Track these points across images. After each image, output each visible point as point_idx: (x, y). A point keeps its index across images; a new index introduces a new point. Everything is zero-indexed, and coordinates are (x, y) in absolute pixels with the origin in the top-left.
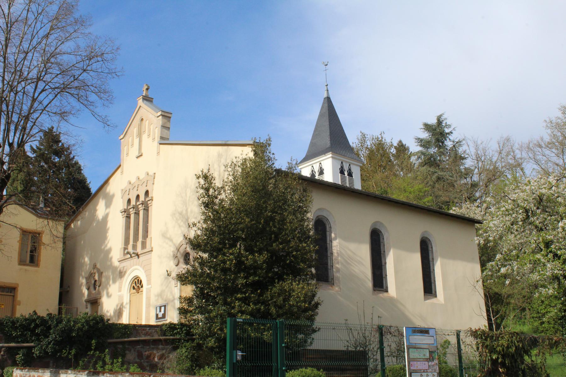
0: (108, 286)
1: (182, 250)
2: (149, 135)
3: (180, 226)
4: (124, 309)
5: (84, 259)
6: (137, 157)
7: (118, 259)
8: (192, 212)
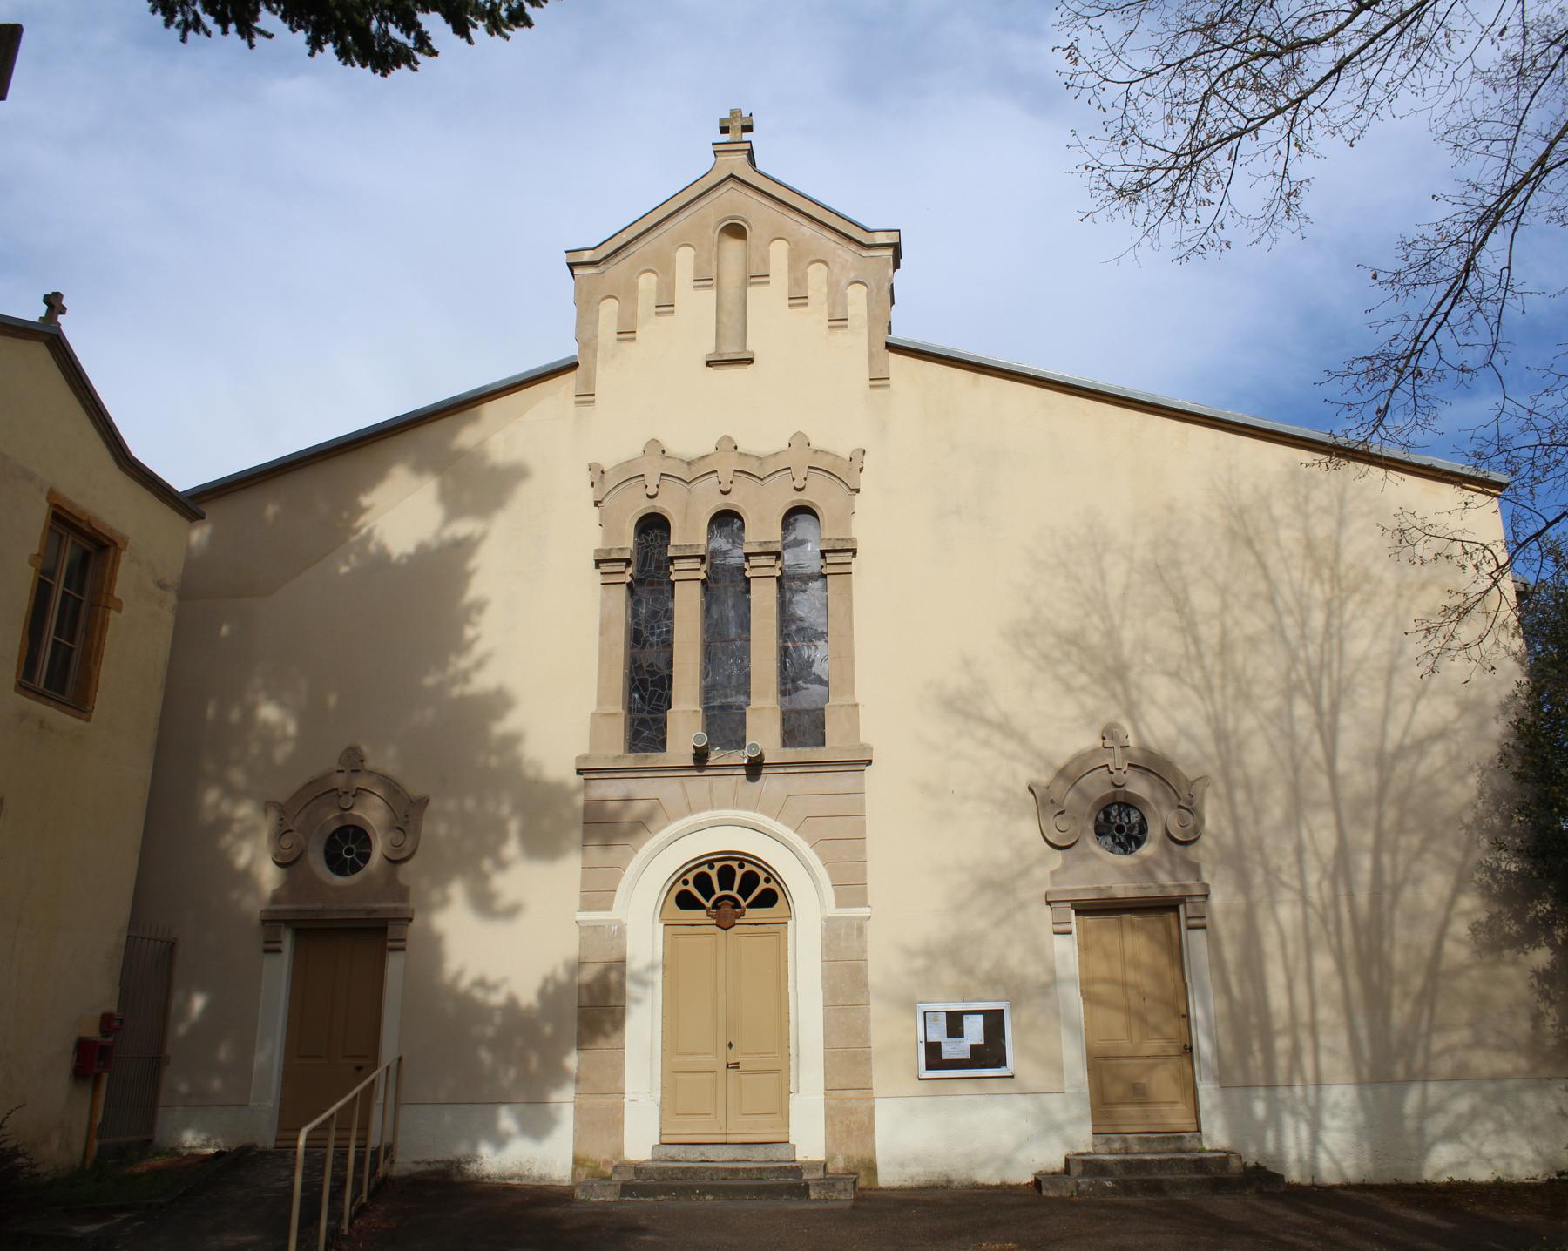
0: (487, 864)
1: (1097, 785)
2: (798, 299)
3: (1069, 689)
4: (631, 988)
5: (249, 712)
6: (709, 364)
7: (585, 758)
8: (1143, 645)
